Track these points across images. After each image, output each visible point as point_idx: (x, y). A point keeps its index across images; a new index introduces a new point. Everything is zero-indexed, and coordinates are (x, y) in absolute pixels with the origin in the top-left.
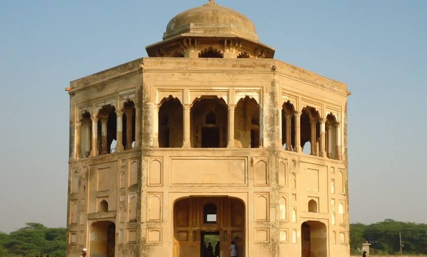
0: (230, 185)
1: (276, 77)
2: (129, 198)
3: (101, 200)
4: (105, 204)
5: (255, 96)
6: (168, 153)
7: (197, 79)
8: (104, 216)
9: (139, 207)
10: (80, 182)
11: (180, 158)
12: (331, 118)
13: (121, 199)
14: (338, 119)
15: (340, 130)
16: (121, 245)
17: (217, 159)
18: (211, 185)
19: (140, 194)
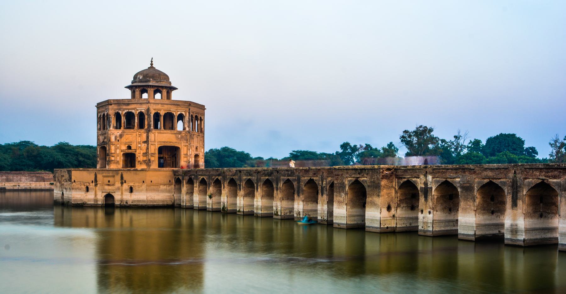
0: (176, 143)
2: (144, 146)
4: (129, 147)
5: (184, 113)
6: (156, 132)
7: (166, 107)
8: (130, 151)
9: (147, 149)
11: (160, 133)
13: (139, 145)
14: (202, 118)
15: (203, 122)
16: (139, 161)
17: (172, 134)
18: (170, 142)
19: (148, 144)
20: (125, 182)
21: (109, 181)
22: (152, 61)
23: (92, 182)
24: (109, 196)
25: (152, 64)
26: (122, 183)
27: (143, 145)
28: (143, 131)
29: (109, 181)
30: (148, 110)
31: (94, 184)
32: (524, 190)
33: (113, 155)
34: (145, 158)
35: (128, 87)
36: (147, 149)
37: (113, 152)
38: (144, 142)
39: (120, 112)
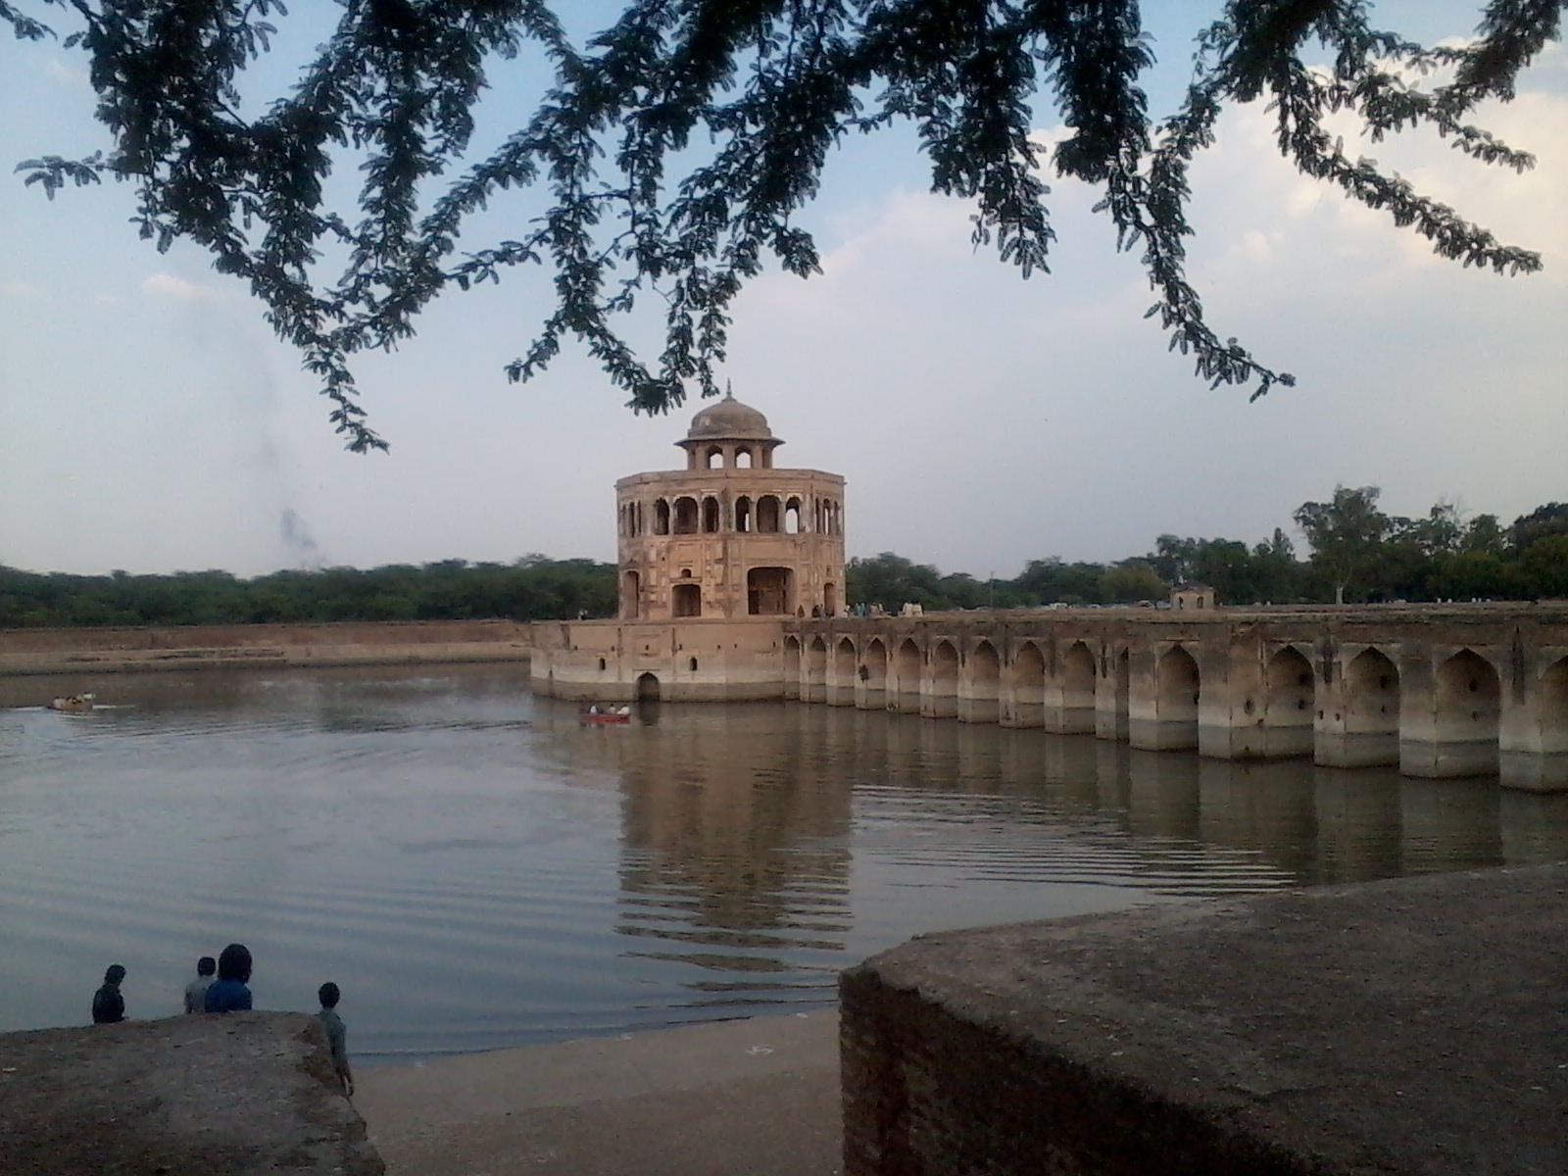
1: (814, 483)
3: (682, 569)
5: (801, 498)
8: (688, 581)
10: (658, 555)
11: (751, 540)
12: (836, 503)
13: (708, 568)
15: (840, 512)
16: (709, 603)
17: (775, 541)
20: (681, 648)
21: (647, 647)
22: (729, 387)
23: (613, 649)
24: (647, 678)
25: (729, 393)
26: (674, 651)
27: (716, 567)
28: (714, 536)
29: (647, 647)
30: (725, 493)
31: (615, 653)
32: (1540, 669)
33: (654, 589)
34: (720, 596)
35: (682, 444)
36: (725, 574)
37: (653, 583)
38: (718, 561)
39: (667, 499)
